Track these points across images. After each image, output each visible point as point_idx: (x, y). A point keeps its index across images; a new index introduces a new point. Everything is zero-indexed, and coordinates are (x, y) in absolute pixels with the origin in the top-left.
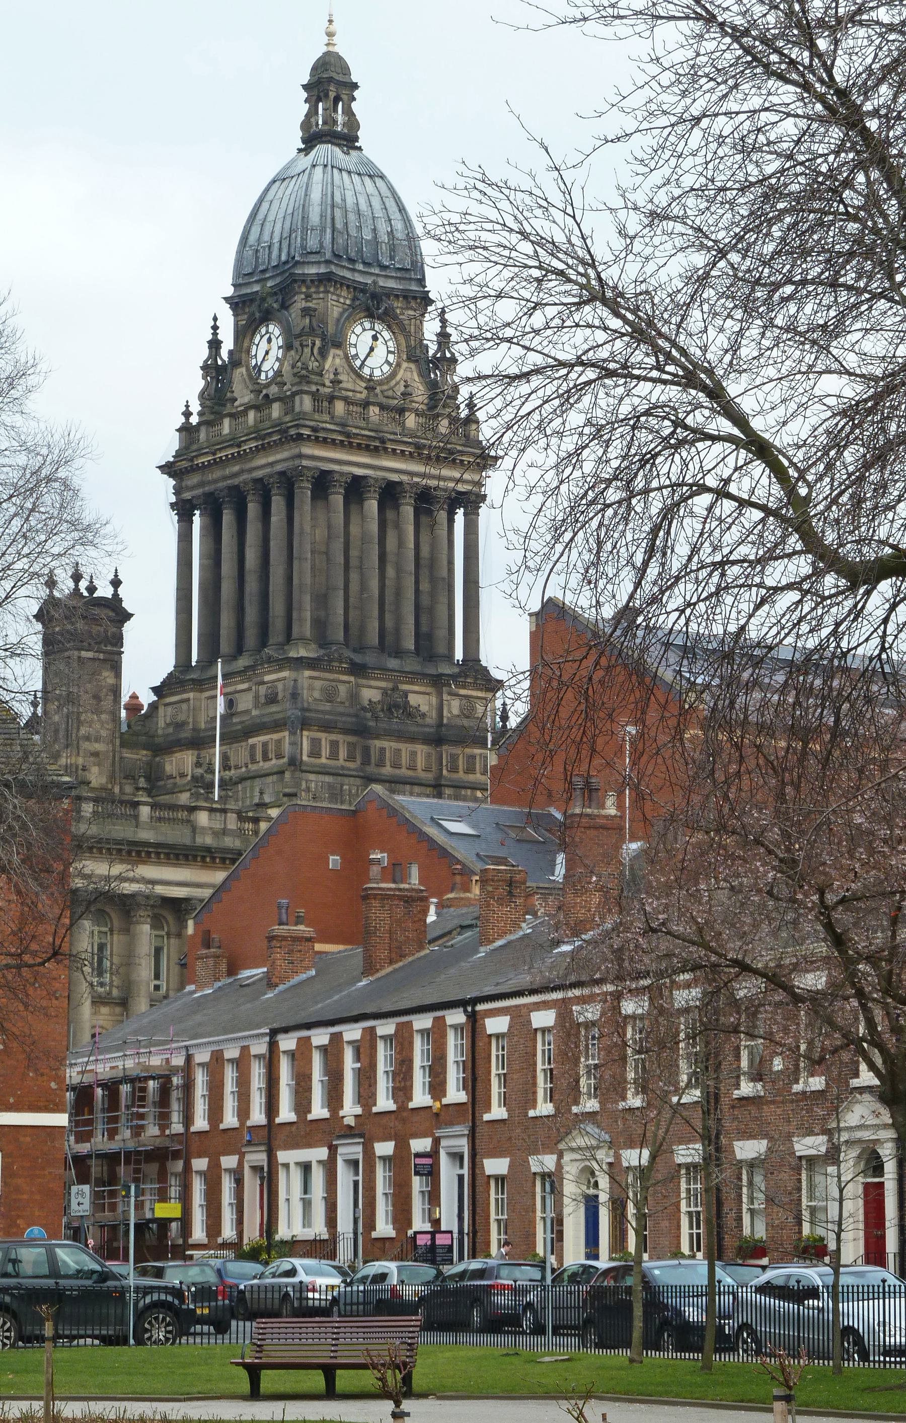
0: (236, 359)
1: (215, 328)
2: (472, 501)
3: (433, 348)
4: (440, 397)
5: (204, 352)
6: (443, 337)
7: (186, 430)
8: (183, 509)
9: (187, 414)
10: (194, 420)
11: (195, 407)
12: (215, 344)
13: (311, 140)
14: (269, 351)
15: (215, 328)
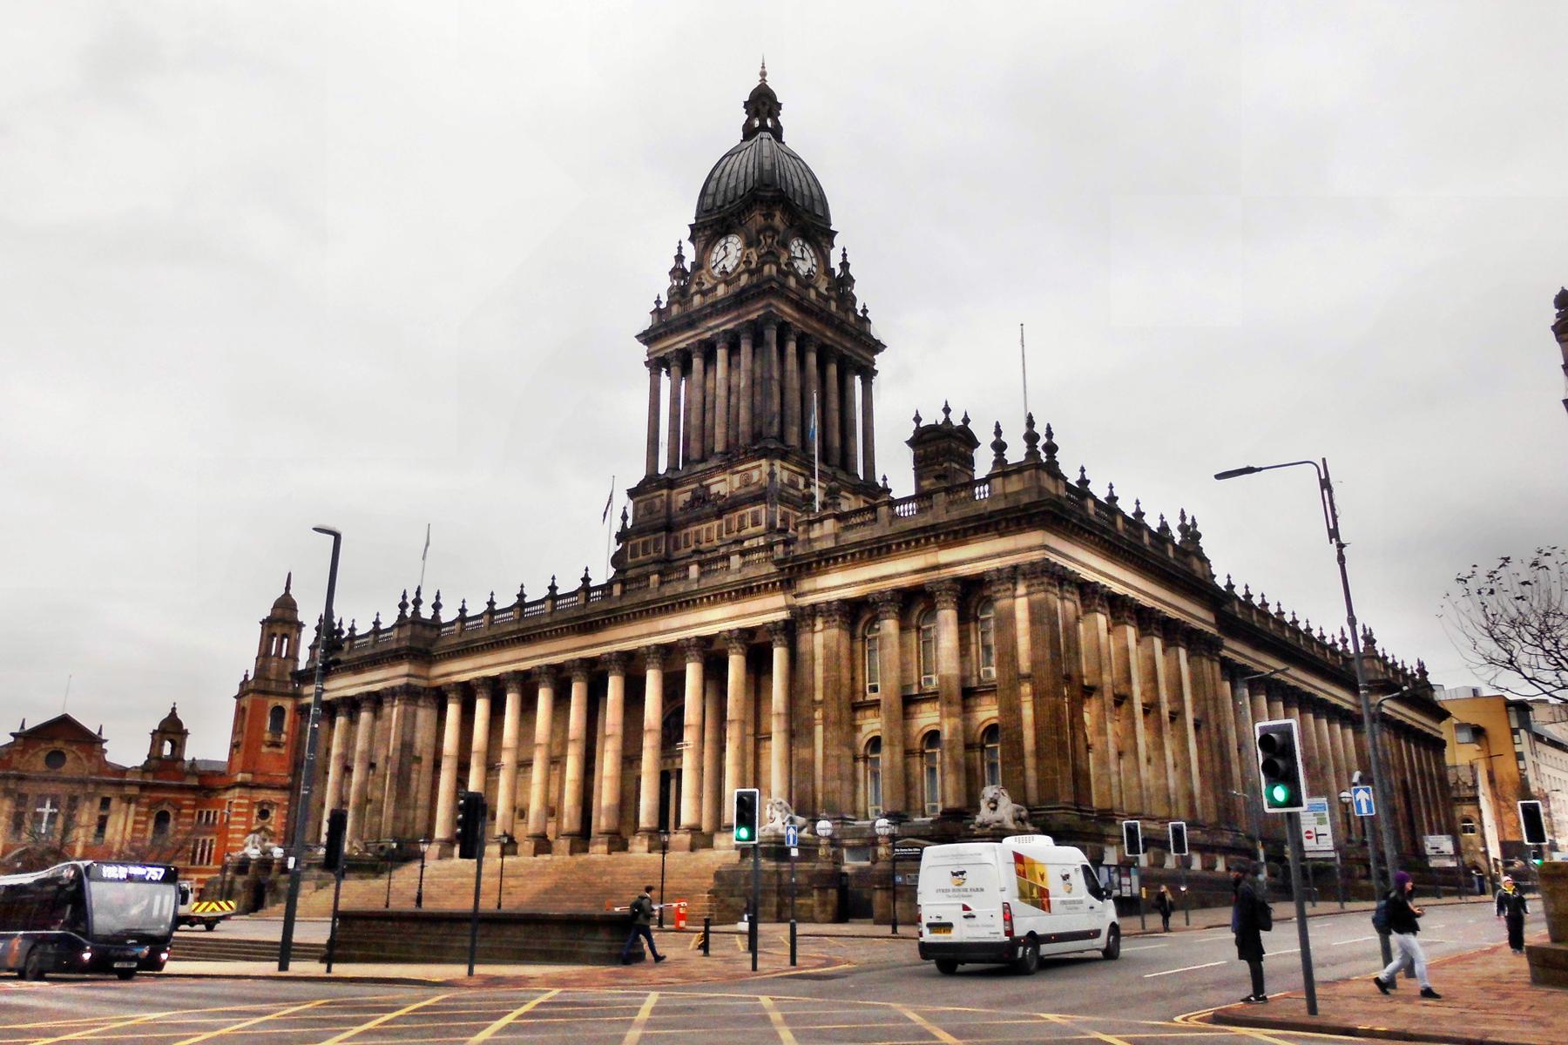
0: (698, 266)
1: (680, 248)
2: (868, 374)
3: (838, 272)
4: (847, 300)
5: (672, 263)
6: (845, 265)
7: (658, 312)
8: (656, 365)
9: (658, 302)
10: (663, 306)
11: (665, 300)
12: (680, 258)
13: (749, 132)
14: (730, 253)
15: (680, 248)
